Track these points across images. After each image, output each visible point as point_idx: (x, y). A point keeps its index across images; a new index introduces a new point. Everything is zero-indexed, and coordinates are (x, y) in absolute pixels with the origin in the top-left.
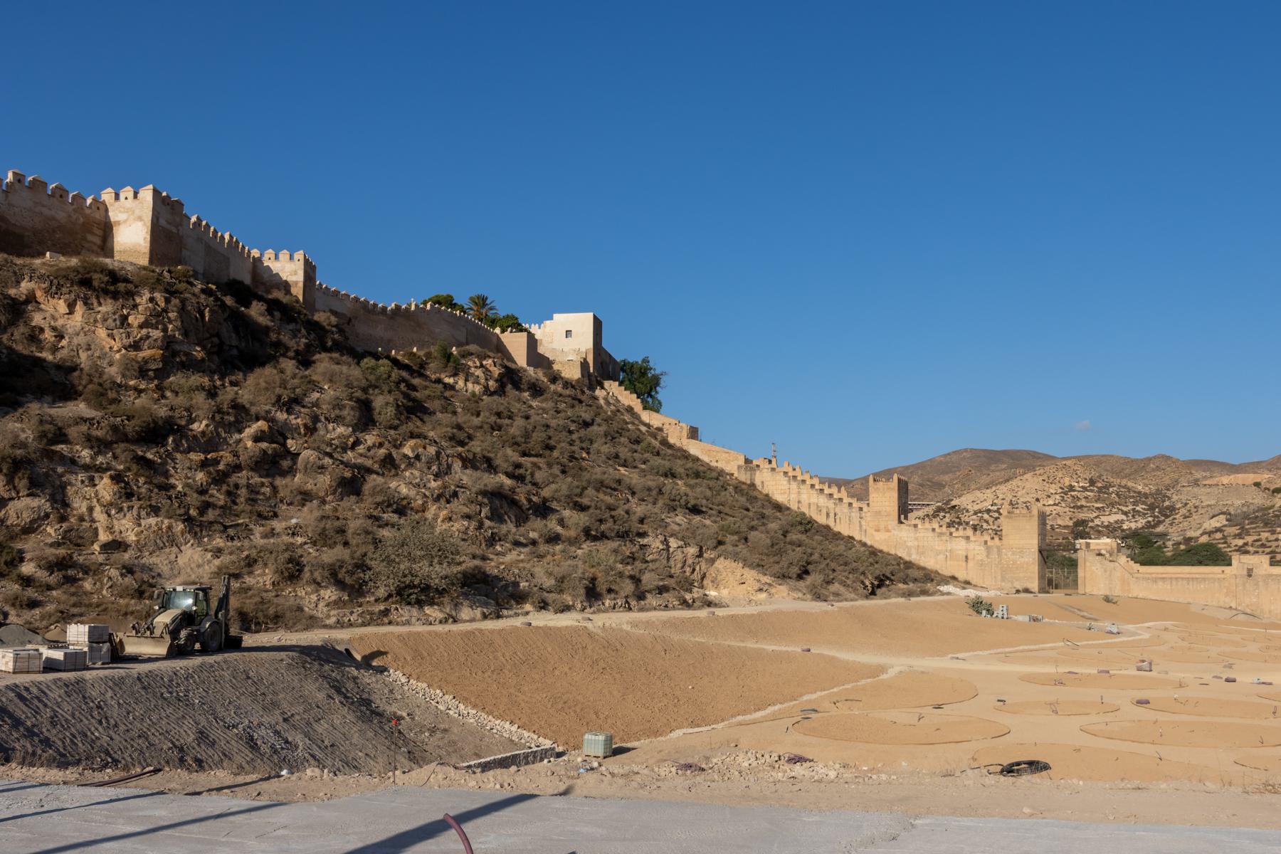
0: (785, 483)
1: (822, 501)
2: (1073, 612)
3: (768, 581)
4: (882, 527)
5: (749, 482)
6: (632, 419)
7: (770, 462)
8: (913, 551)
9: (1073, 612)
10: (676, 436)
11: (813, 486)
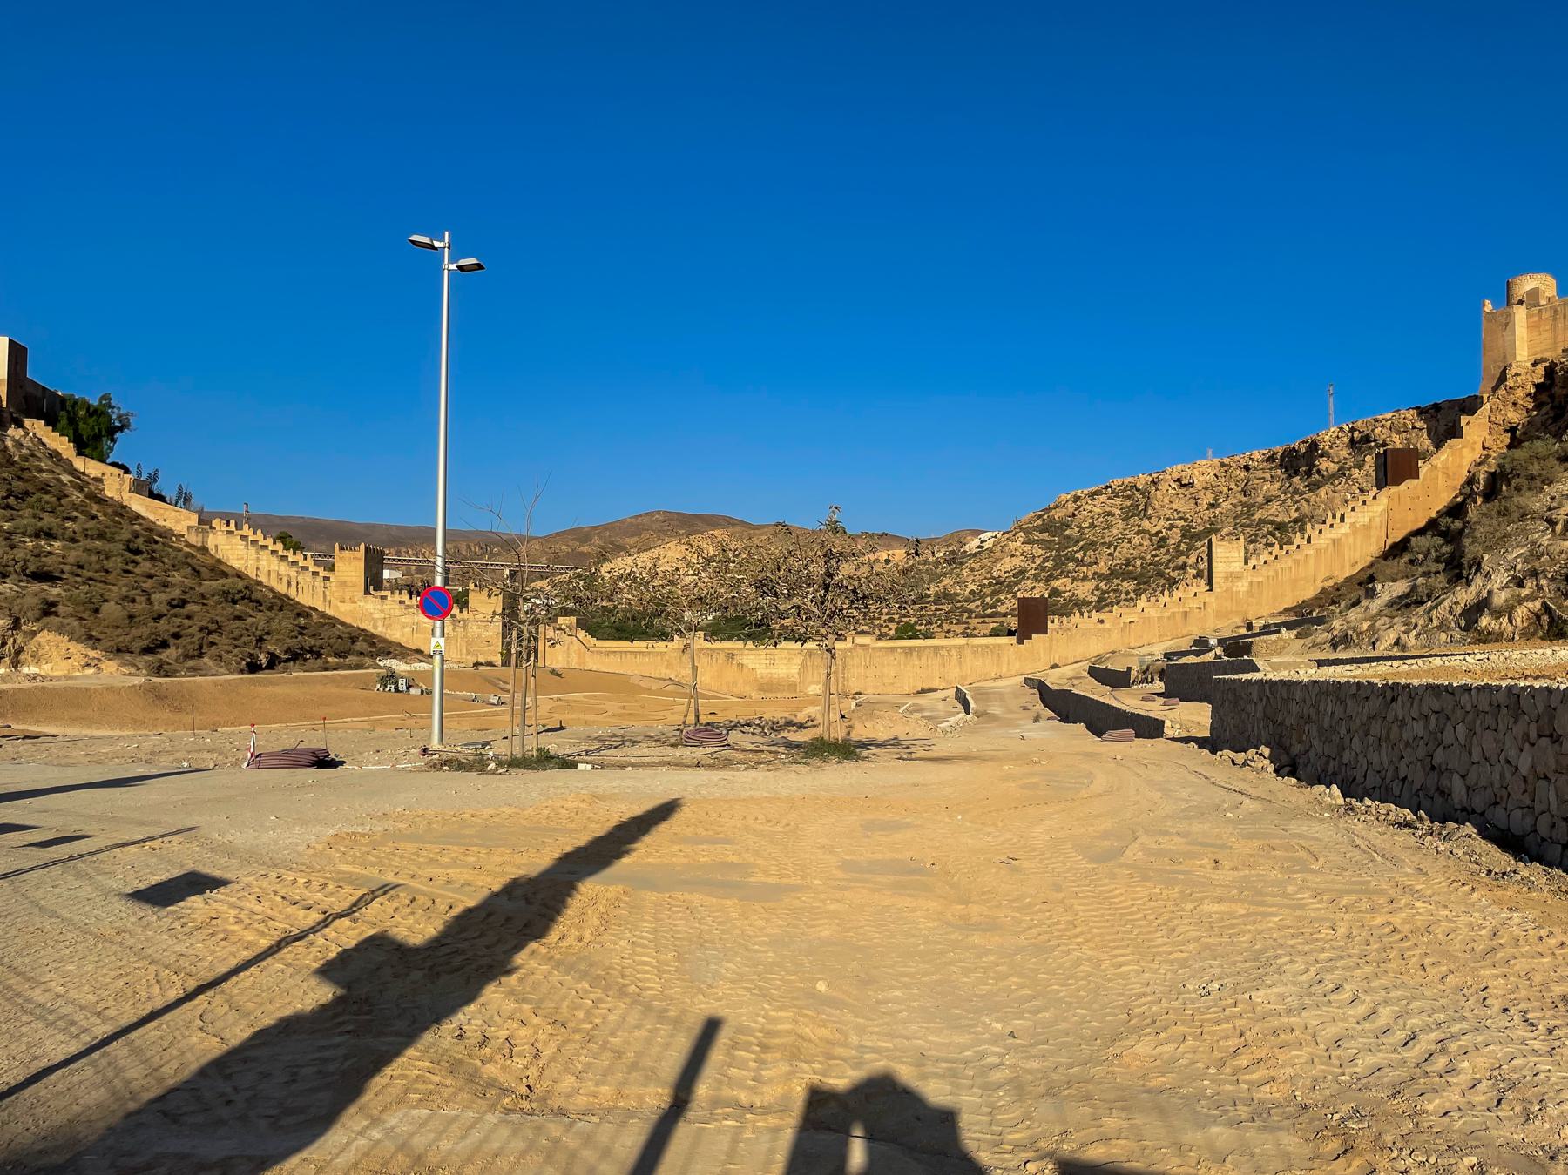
0: (243, 547)
1: (284, 568)
2: (495, 685)
3: (96, 656)
4: (347, 598)
5: (199, 545)
6: (53, 466)
7: (228, 524)
9: (495, 685)
10: (116, 487)
11: (274, 552)
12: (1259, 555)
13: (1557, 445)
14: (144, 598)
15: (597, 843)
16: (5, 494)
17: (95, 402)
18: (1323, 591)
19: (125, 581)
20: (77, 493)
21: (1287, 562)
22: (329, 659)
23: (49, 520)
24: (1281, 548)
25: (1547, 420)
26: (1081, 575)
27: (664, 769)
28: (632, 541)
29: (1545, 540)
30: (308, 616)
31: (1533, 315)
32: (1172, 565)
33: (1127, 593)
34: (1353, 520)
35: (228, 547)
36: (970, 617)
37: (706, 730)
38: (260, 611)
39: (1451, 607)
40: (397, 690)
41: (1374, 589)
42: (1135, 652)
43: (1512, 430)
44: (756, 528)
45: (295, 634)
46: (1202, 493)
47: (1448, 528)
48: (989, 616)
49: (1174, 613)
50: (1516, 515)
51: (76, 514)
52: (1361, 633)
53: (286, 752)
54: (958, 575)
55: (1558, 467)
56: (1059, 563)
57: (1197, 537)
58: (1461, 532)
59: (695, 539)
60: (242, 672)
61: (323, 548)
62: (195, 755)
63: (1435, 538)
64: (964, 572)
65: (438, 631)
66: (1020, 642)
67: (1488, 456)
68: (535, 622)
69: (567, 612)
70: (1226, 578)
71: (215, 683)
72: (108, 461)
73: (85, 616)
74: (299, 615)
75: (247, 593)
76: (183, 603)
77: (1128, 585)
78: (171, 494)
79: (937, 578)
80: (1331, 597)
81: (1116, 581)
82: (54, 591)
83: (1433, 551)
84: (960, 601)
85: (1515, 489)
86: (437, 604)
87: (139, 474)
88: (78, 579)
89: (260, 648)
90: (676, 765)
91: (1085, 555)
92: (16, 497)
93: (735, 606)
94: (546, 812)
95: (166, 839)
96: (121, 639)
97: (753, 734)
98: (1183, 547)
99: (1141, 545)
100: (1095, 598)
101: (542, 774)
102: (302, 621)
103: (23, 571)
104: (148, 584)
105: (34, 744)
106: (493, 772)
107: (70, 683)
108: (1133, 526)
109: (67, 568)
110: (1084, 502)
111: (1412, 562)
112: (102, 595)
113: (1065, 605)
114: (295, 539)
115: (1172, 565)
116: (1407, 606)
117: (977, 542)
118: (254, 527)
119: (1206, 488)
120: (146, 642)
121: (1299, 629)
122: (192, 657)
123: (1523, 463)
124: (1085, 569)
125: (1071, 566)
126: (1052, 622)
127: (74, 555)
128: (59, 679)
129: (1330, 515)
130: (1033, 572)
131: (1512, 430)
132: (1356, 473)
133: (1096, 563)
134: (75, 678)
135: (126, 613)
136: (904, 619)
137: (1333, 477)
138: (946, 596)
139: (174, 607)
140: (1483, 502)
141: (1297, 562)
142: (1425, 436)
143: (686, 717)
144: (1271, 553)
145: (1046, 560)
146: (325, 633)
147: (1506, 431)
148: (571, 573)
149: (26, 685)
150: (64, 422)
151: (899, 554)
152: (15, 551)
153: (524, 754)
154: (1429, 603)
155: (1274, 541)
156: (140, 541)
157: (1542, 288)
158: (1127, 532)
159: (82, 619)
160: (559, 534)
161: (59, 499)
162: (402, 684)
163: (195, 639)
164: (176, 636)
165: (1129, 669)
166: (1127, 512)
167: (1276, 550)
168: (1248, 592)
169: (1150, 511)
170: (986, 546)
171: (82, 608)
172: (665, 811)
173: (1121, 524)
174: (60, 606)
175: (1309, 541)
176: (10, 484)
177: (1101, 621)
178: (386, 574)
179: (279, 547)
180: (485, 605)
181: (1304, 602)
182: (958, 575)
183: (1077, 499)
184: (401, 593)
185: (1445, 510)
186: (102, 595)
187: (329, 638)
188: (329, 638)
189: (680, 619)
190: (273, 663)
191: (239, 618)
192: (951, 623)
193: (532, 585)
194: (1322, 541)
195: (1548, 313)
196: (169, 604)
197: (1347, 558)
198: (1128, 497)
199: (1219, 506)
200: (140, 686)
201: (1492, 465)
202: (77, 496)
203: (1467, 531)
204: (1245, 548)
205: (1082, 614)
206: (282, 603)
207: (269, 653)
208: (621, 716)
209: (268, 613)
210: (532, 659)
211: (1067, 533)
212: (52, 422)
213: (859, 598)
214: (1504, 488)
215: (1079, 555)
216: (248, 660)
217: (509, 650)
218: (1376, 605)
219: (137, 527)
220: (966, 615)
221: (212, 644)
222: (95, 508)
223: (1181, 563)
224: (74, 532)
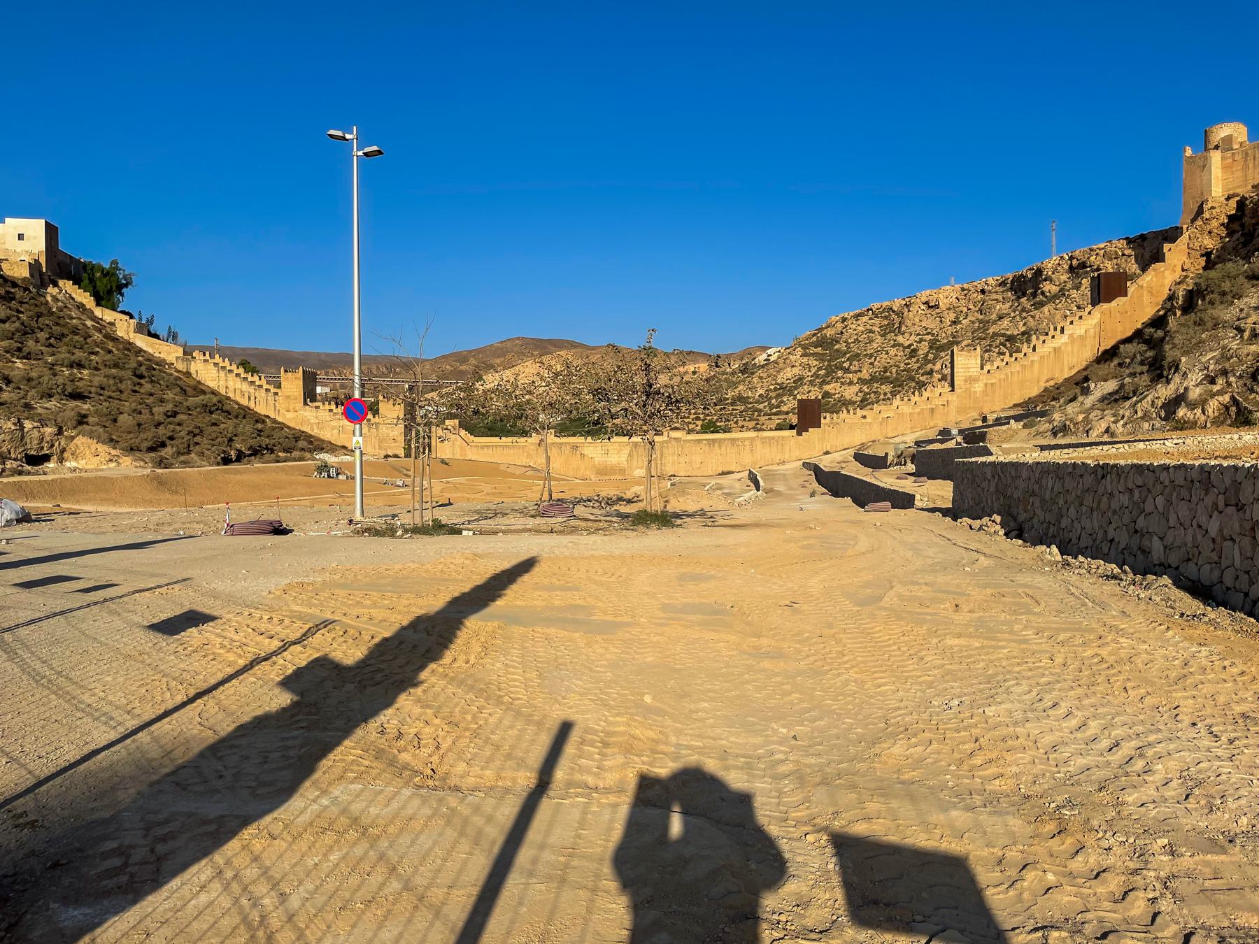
5: (185, 370)
7: (204, 355)
8: (315, 427)
10: (125, 329)
11: (238, 375)
12: (993, 362)
13: (1246, 265)
14: (147, 411)
15: (477, 589)
16: (48, 336)
17: (107, 266)
18: (1046, 390)
19: (133, 398)
20: (97, 334)
21: (1016, 367)
22: (280, 454)
23: (79, 355)
24: (1011, 356)
25: (1237, 245)
26: (848, 381)
27: (527, 534)
28: (498, 361)
29: (1234, 345)
30: (263, 422)
31: (1227, 158)
32: (921, 371)
33: (885, 394)
34: (1070, 332)
35: (206, 372)
36: (759, 415)
37: (558, 505)
38: (230, 419)
39: (1153, 401)
40: (329, 476)
41: (1088, 387)
42: (891, 441)
43: (1207, 255)
44: (593, 348)
45: (255, 435)
46: (946, 313)
47: (1152, 337)
48: (775, 414)
49: (923, 409)
50: (1209, 325)
51: (97, 349)
52: (1077, 423)
53: (252, 523)
54: (750, 382)
55: (1247, 284)
56: (830, 372)
57: (942, 348)
58: (1162, 340)
59: (546, 359)
60: (218, 464)
61: (273, 371)
62: (188, 526)
63: (1140, 345)
64: (754, 380)
65: (357, 432)
66: (799, 434)
67: (1186, 277)
68: (429, 424)
69: (451, 416)
70: (966, 381)
71: (200, 473)
72: (119, 310)
73: (107, 424)
74: (257, 421)
75: (219, 406)
76: (175, 414)
77: (886, 388)
78: (163, 333)
79: (734, 385)
80: (1053, 394)
81: (876, 385)
82: (85, 407)
83: (1138, 356)
84: (751, 403)
85: (1209, 303)
86: (356, 411)
87: (140, 319)
88: (101, 397)
89: (231, 446)
90: (536, 531)
91: (851, 364)
92: (56, 338)
93: (577, 409)
94: (440, 567)
95: (170, 587)
96: (133, 441)
97: (593, 507)
98: (931, 356)
99: (896, 355)
100: (859, 399)
101: (435, 538)
102: (260, 426)
103: (63, 392)
104: (150, 400)
105: (76, 518)
106: (400, 537)
107: (99, 473)
108: (890, 340)
109: (93, 390)
110: (850, 322)
111: (1120, 365)
112: (118, 409)
113: (835, 404)
114: (252, 365)
115: (921, 371)
116: (1116, 401)
117: (764, 356)
118: (223, 357)
119: (949, 309)
120: (150, 443)
121: (1025, 421)
122: (183, 454)
123: (1216, 281)
124: (851, 375)
125: (840, 373)
126: (825, 418)
127: (98, 380)
128: (91, 470)
129: (1052, 328)
130: (809, 379)
131: (1207, 255)
132: (1074, 293)
133: (859, 371)
134: (100, 470)
135: (135, 422)
136: (708, 418)
137: (1055, 297)
138: (741, 399)
139: (169, 417)
140: (1182, 315)
141: (1024, 367)
142: (1133, 261)
143: (542, 495)
144: (1002, 360)
145: (820, 369)
146: (277, 434)
147: (1202, 255)
148: (454, 386)
149: (69, 475)
150: (86, 282)
151: (703, 367)
152: (57, 377)
153: (423, 525)
154: (1135, 399)
155: (1005, 350)
156: (143, 368)
157: (1236, 135)
158: (885, 345)
159: (105, 427)
160: (444, 357)
161: (85, 339)
162: (333, 472)
163: (185, 440)
164: (171, 438)
165: (887, 454)
166: (885, 330)
167: (1007, 358)
168: (983, 392)
169: (903, 328)
170: (772, 359)
171: (105, 419)
172: (527, 566)
173: (880, 339)
174: (90, 418)
175: (1034, 349)
176: (51, 328)
177: (864, 417)
178: (319, 390)
179: (241, 370)
180: (391, 411)
181: (1029, 399)
182: (750, 382)
183: (844, 320)
184: (330, 404)
185: (1149, 322)
186: (118, 409)
187: (279, 438)
188: (279, 438)
189: (536, 420)
190: (240, 457)
191: (215, 424)
192: (745, 420)
193: (426, 396)
194: (1046, 350)
195: (1241, 154)
196: (165, 414)
197: (1066, 363)
198: (886, 318)
199: (960, 323)
200: (148, 476)
201: (1190, 284)
202: (97, 336)
203: (1167, 339)
204: (981, 357)
205: (848, 412)
206: (245, 413)
207: (237, 450)
208: (493, 494)
209: (235, 420)
210: (427, 452)
211: (836, 347)
212: (77, 282)
213: (672, 401)
214: (1200, 302)
215: (846, 365)
216: (223, 455)
217: (410, 446)
218: (1089, 401)
219: (140, 358)
220: (756, 413)
221: (197, 444)
222: (110, 345)
223: (928, 369)
224: (97, 363)
